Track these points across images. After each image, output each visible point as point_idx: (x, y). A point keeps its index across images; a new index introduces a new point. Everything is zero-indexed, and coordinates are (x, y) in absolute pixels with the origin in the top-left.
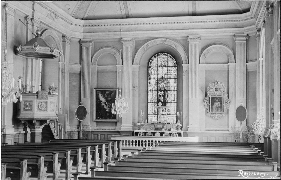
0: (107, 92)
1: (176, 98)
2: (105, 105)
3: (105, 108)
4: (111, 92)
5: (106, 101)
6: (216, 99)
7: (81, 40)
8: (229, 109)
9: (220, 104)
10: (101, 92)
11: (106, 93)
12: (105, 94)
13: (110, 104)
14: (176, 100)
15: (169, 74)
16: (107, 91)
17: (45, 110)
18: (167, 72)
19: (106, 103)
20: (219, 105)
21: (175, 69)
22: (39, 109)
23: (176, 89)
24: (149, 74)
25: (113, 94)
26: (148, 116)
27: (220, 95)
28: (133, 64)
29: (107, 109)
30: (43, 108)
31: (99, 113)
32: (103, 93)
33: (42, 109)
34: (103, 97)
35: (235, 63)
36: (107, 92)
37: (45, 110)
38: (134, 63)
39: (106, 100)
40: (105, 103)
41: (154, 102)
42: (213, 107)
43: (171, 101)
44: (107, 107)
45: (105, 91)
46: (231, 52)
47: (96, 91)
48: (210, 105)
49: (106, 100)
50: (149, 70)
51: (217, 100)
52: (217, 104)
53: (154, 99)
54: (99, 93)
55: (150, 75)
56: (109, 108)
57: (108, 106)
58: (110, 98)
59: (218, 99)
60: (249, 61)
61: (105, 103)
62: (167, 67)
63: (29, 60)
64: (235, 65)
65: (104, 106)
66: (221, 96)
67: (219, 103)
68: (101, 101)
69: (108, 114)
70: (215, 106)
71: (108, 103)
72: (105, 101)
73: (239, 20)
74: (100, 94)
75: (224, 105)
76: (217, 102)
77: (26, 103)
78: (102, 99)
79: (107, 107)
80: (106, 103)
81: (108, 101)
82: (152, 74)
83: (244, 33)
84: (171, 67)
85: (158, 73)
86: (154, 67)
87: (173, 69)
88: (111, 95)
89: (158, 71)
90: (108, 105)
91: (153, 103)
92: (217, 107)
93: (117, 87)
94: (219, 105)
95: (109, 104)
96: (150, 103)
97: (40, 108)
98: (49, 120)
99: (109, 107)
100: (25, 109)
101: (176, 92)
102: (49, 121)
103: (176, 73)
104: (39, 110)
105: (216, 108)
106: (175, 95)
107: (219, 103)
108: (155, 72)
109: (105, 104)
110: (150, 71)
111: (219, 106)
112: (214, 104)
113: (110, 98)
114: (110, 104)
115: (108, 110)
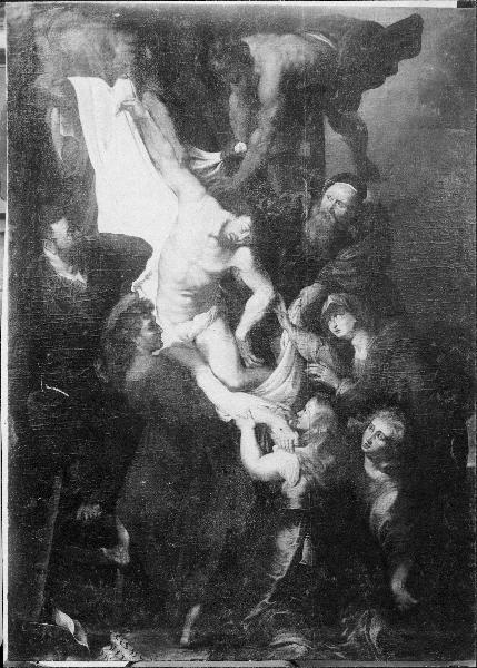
3: (230, 405)
5: (244, 259)
10: (122, 48)
13: (341, 325)
19: (254, 311)
29: (281, 432)
31: (90, 511)
39: (241, 226)
40: (226, 295)
44: (281, 382)
49: (241, 226)
56: (313, 408)
57: (302, 361)
61: (226, 295)
69: (289, 541)
71: (286, 293)
72: (228, 245)
80: (254, 311)
88: (371, 105)
90: (290, 340)
95: (314, 323)
99: (310, 389)
109: (232, 325)
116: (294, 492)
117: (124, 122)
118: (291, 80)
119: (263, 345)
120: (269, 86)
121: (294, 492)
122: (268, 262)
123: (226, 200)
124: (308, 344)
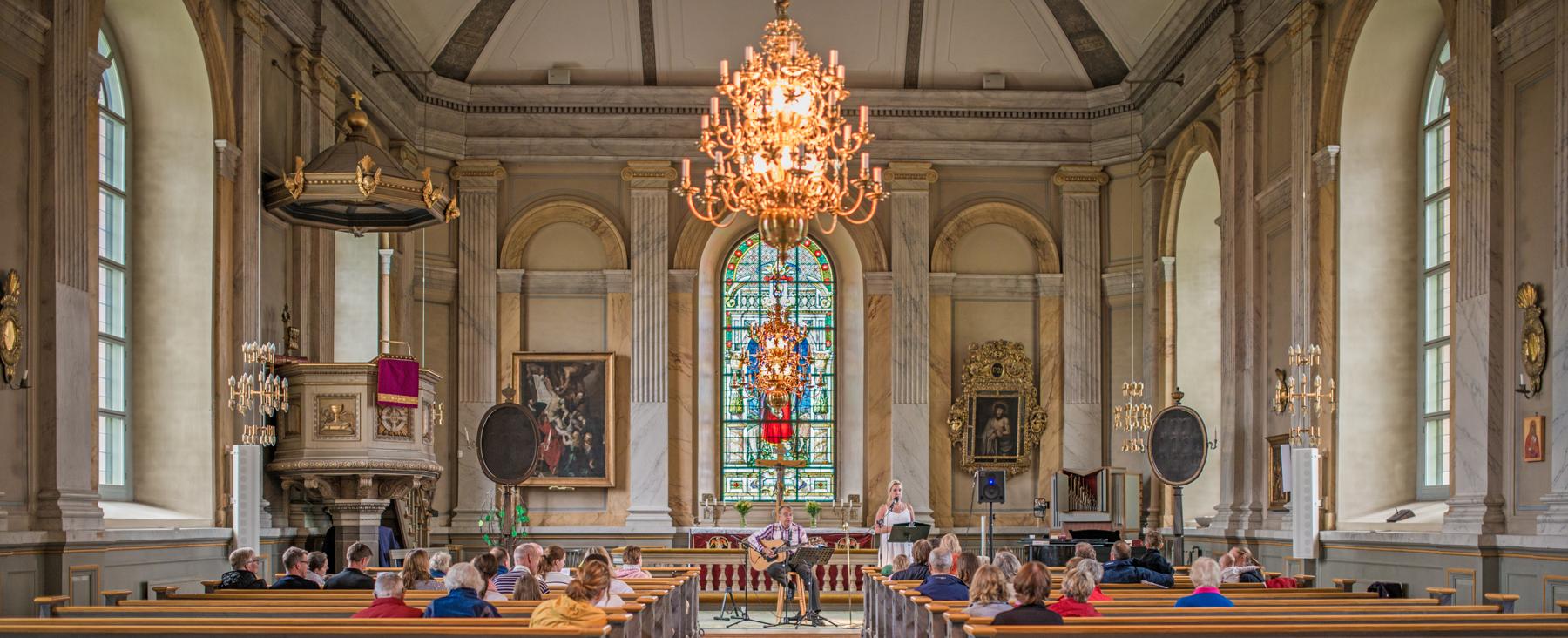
0: (568, 371)
1: (830, 401)
2: (558, 420)
3: (562, 432)
4: (584, 369)
5: (563, 406)
6: (997, 407)
7: (454, 163)
8: (1039, 446)
9: (1007, 427)
10: (542, 370)
11: (563, 371)
12: (559, 378)
13: (580, 418)
14: (831, 410)
15: (805, 309)
16: (570, 364)
17: (405, 432)
18: (797, 304)
20: (1004, 429)
21: (825, 292)
22: (382, 430)
23: (829, 370)
24: (725, 309)
25: (590, 378)
26: (835, 468)
27: (1012, 393)
28: (671, 267)
30: (397, 425)
32: (552, 370)
33: (396, 429)
34: (551, 387)
35: (1061, 272)
36: (568, 371)
37: (405, 432)
38: (501, 265)
39: (563, 400)
40: (559, 413)
41: (744, 417)
42: (984, 438)
43: (813, 415)
44: (569, 428)
45: (560, 365)
46: (1045, 234)
47: (524, 364)
48: (970, 430)
49: (563, 400)
50: (726, 293)
51: (999, 412)
52: (999, 425)
53: (745, 408)
54: (533, 372)
55: (729, 316)
56: (575, 433)
57: (573, 425)
58: (580, 394)
59: (1003, 407)
60: (1109, 269)
61: (559, 413)
62: (797, 282)
63: (306, 233)
64: (1062, 279)
65: (554, 423)
66: (1013, 396)
67: (1006, 420)
68: (544, 405)
69: (571, 456)
70: (989, 434)
71: (571, 412)
72: (560, 404)
73: (1074, 115)
74: (538, 378)
75: (1022, 430)
76: (999, 419)
77: (325, 403)
78: (547, 396)
79: (569, 428)
81: (571, 406)
82: (738, 308)
83: (1094, 163)
84: (811, 282)
85: (760, 305)
86: (746, 282)
87: (818, 292)
88: (585, 379)
89: (760, 297)
91: (741, 421)
92: (997, 438)
93: (609, 350)
94: (1004, 429)
96: (731, 421)
97: (386, 424)
98: (421, 476)
99: (575, 429)
100: (321, 432)
101: (829, 380)
102: (421, 480)
103: (831, 309)
104: (382, 433)
105: (993, 441)
106: (828, 394)
107: (1006, 420)
108: (751, 301)
110: (731, 297)
111: (1006, 433)
112: (988, 427)
113: (580, 394)
114: (580, 418)
115: (570, 442)
116: (572, 448)
117: (542, 383)
118: (572, 376)
119: (566, 422)
120: (567, 376)
121: (572, 448)
122: (567, 408)
123: (560, 396)
124: (575, 421)
